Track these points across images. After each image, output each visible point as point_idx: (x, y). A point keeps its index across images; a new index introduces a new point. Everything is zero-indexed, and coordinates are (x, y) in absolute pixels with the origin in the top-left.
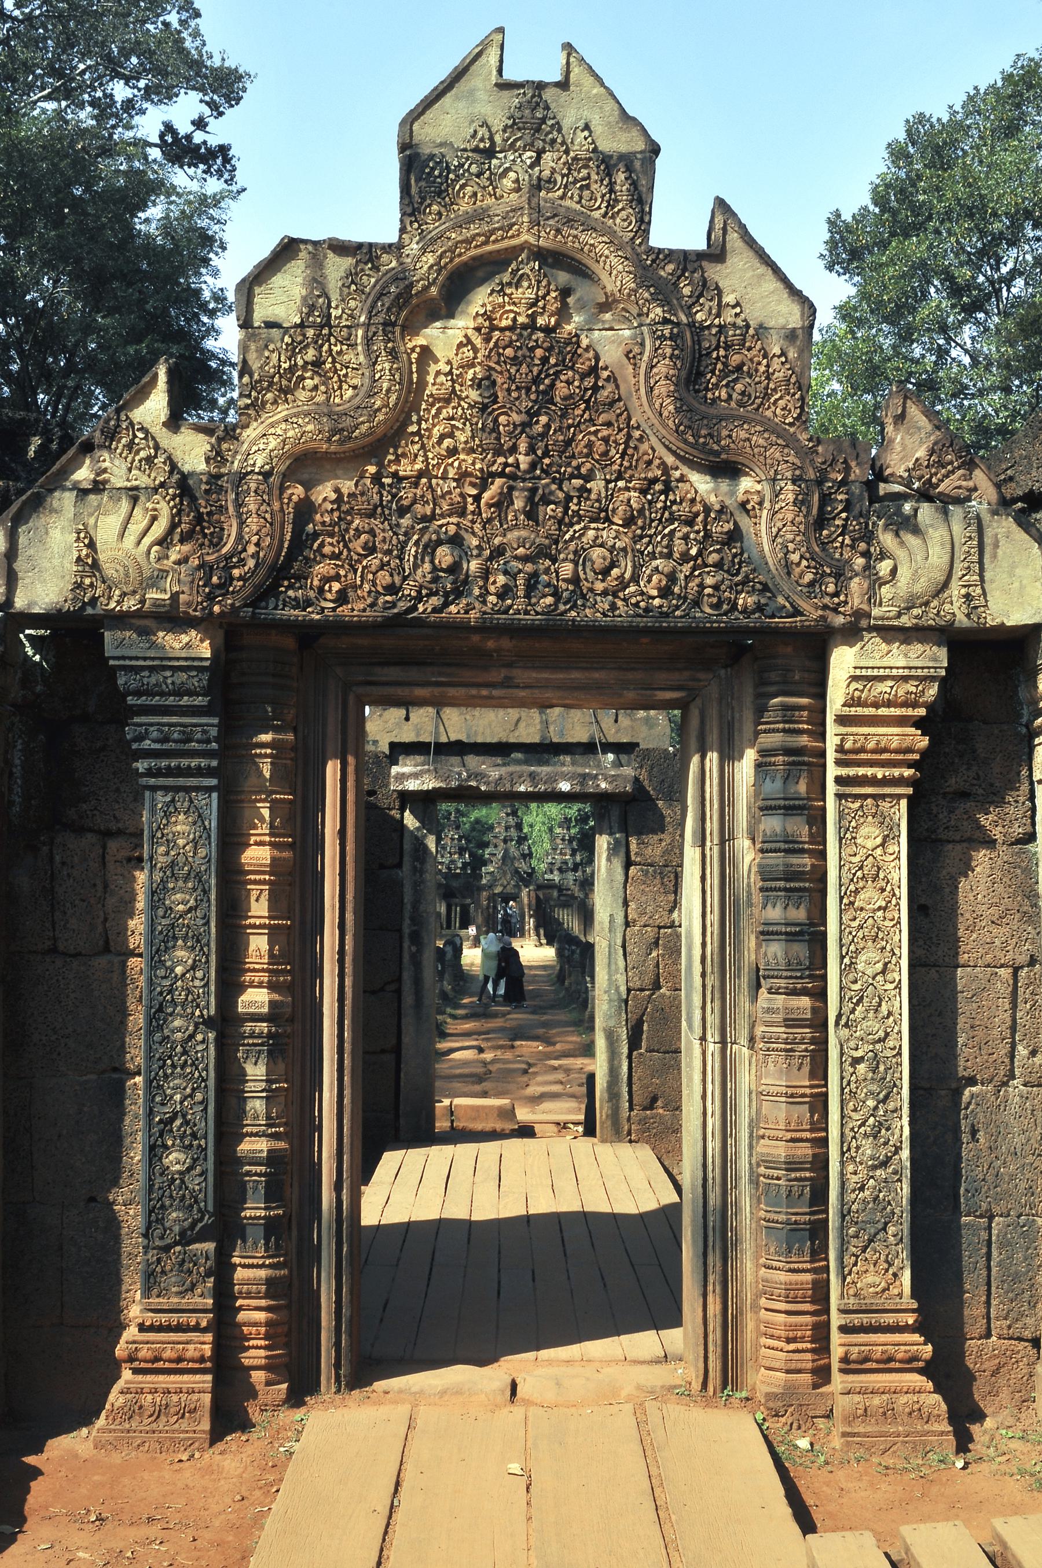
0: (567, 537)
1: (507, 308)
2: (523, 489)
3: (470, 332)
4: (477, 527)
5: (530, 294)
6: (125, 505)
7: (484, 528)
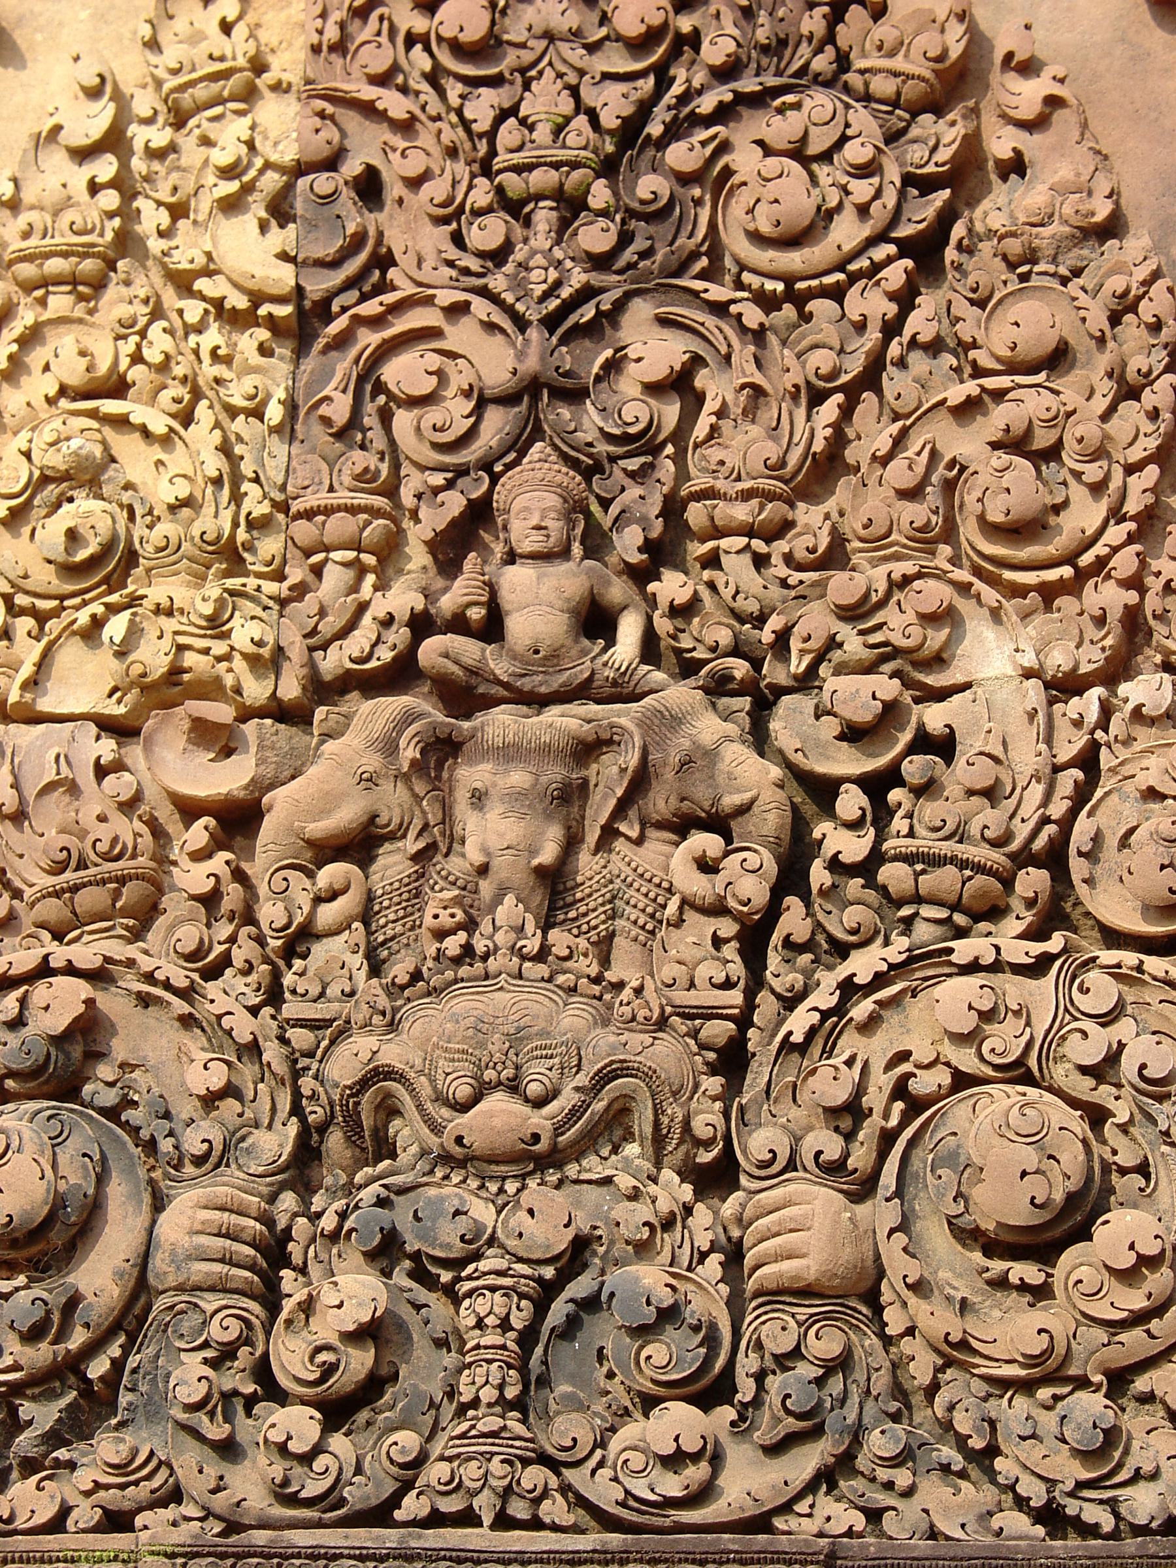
0: (799, 1022)
7: (274, 995)
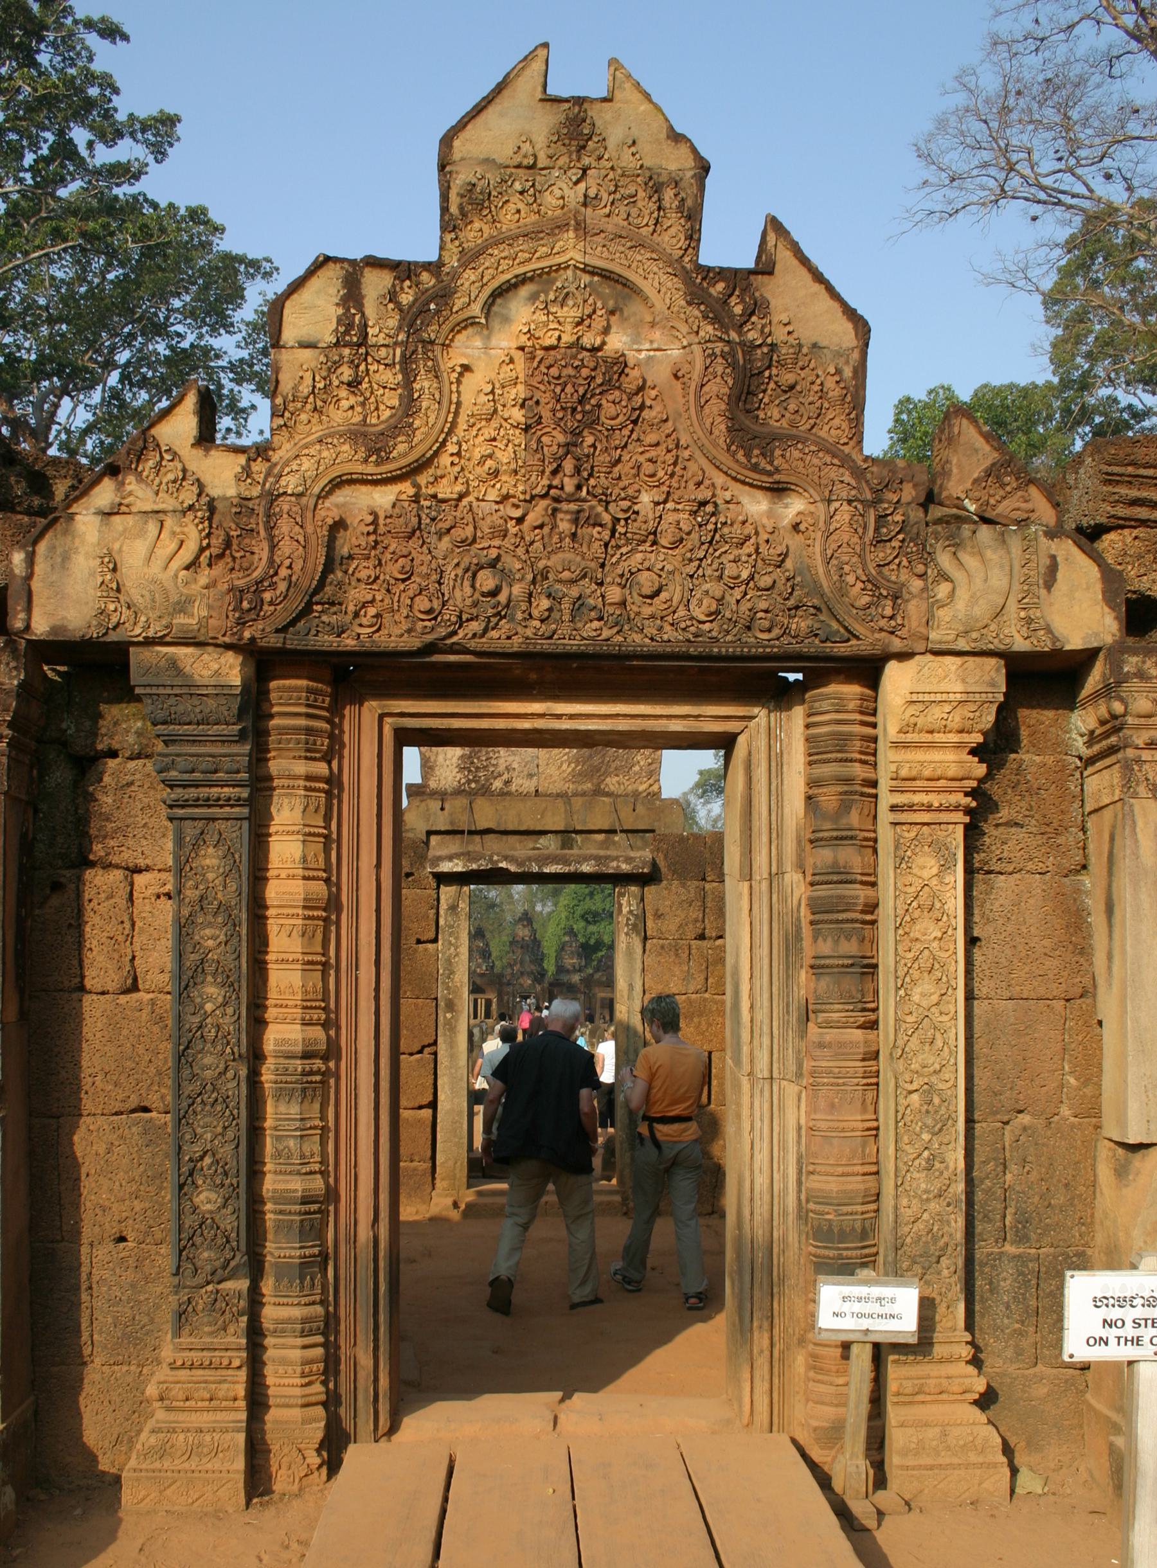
0: (614, 560)
1: (552, 326)
2: (567, 512)
3: (514, 353)
4: (520, 551)
5: (576, 313)
6: (152, 528)
